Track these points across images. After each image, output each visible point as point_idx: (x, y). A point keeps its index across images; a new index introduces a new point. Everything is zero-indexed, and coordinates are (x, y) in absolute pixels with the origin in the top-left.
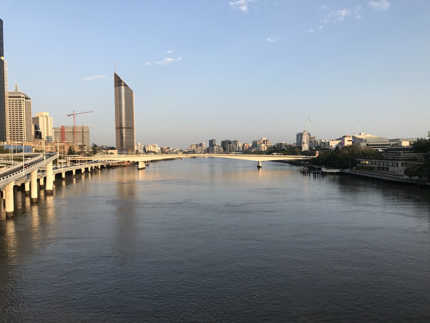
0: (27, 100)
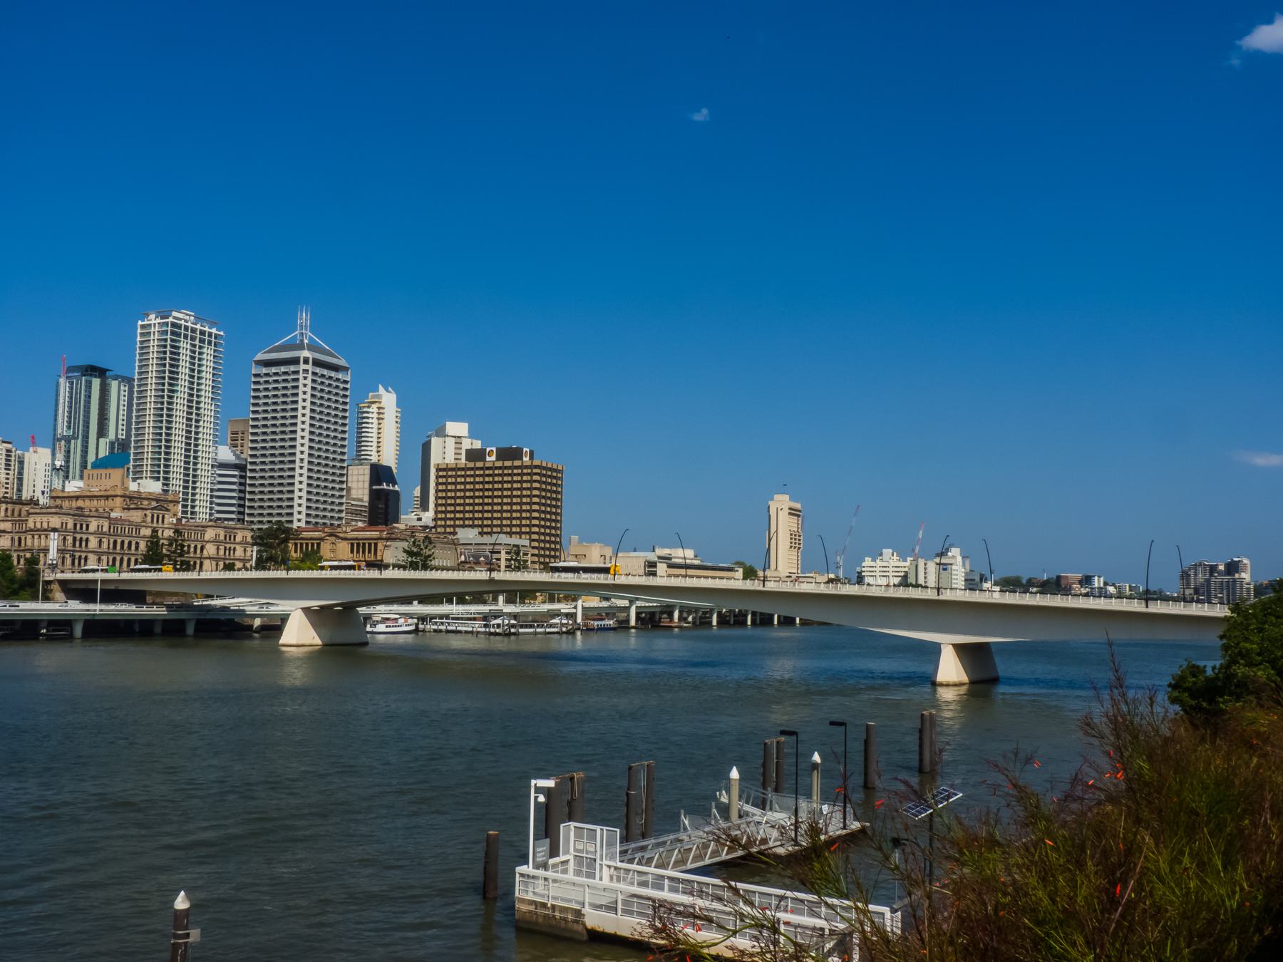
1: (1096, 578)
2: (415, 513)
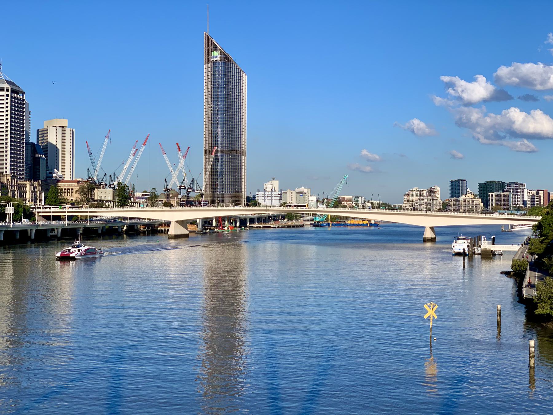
0: (16, 95)
1: (360, 198)
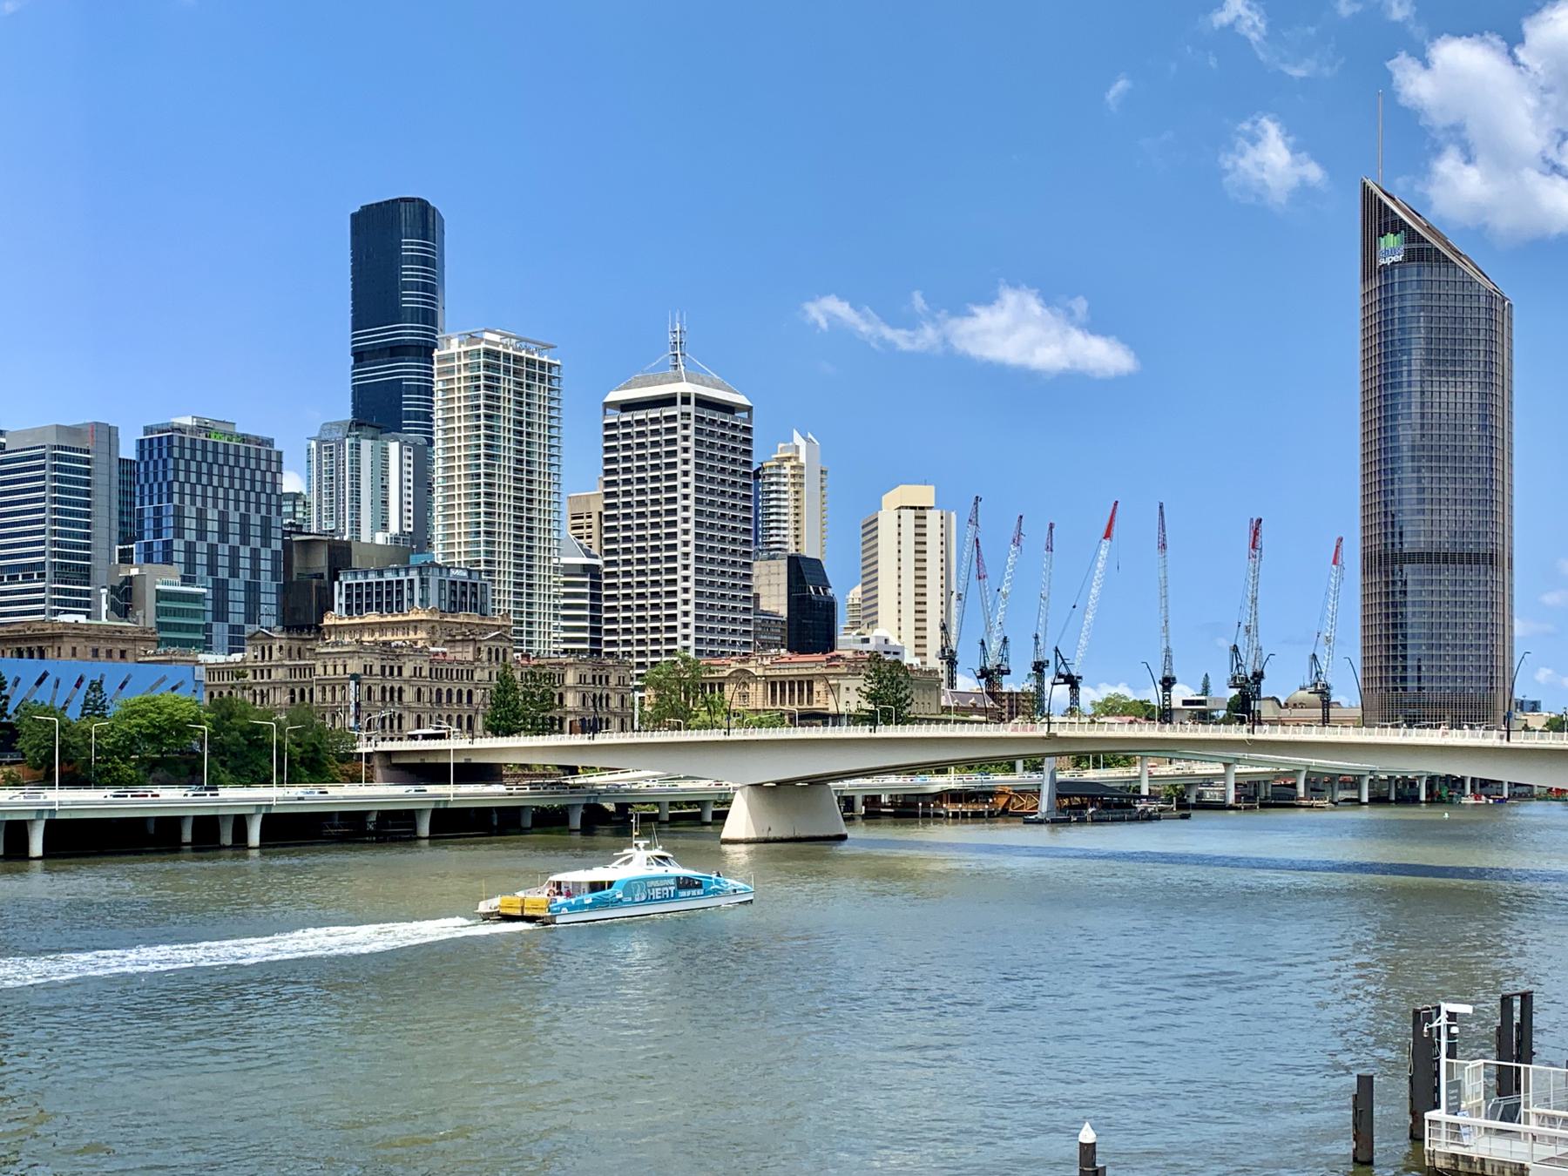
2: (858, 631)
